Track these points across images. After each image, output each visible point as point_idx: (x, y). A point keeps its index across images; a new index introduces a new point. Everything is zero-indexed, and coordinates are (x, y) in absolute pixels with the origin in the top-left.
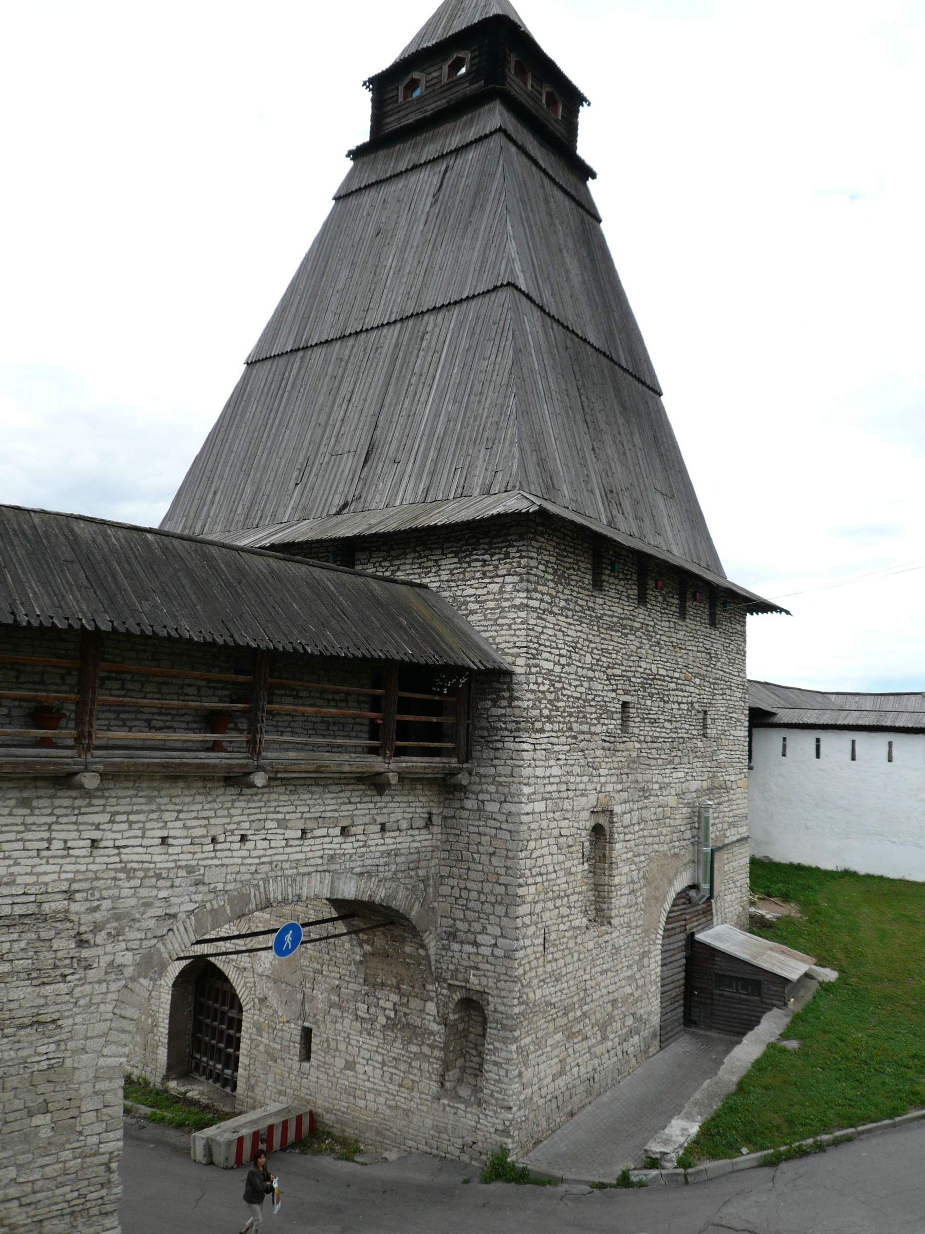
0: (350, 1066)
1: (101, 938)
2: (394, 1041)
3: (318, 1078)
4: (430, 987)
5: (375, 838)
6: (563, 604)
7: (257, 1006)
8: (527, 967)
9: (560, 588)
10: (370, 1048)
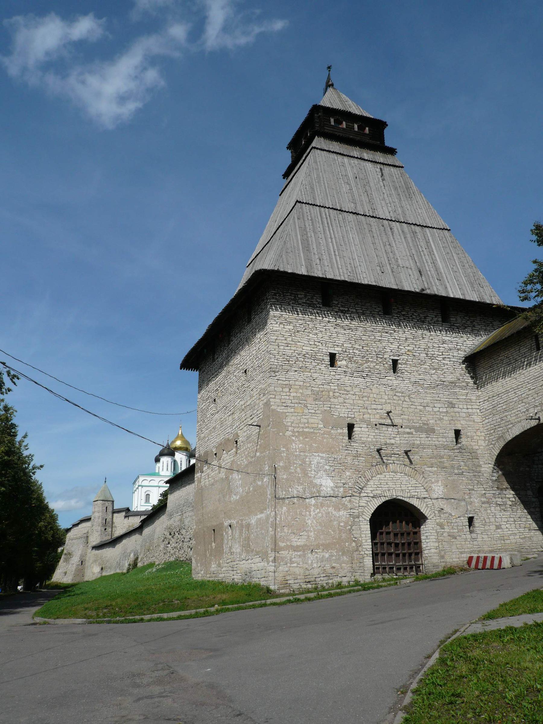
0: (498, 527)
2: (517, 510)
3: (483, 538)
4: (528, 484)
7: (437, 514)
10: (507, 516)
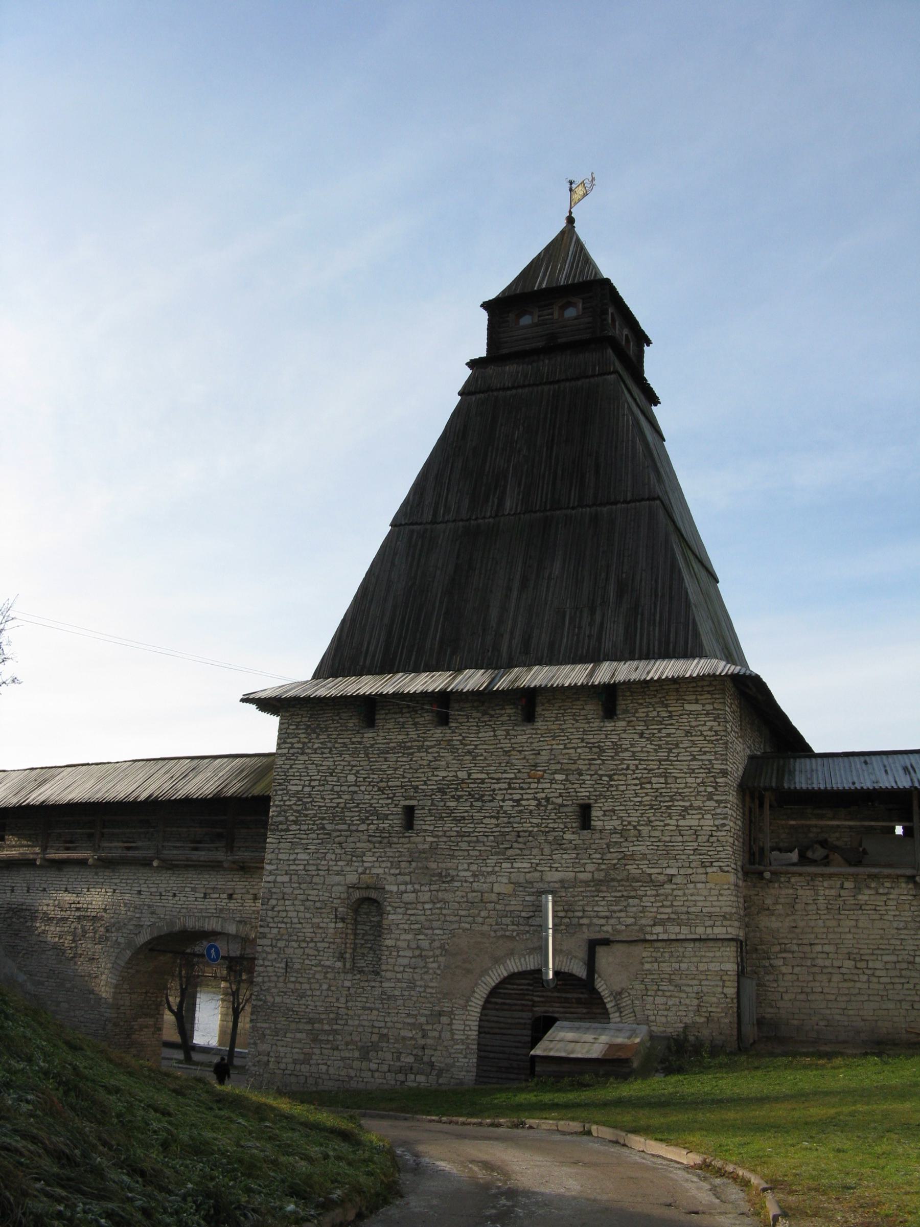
1: (113, 929)
5: (249, 903)
6: (316, 746)
8: (266, 979)
9: (314, 736)
